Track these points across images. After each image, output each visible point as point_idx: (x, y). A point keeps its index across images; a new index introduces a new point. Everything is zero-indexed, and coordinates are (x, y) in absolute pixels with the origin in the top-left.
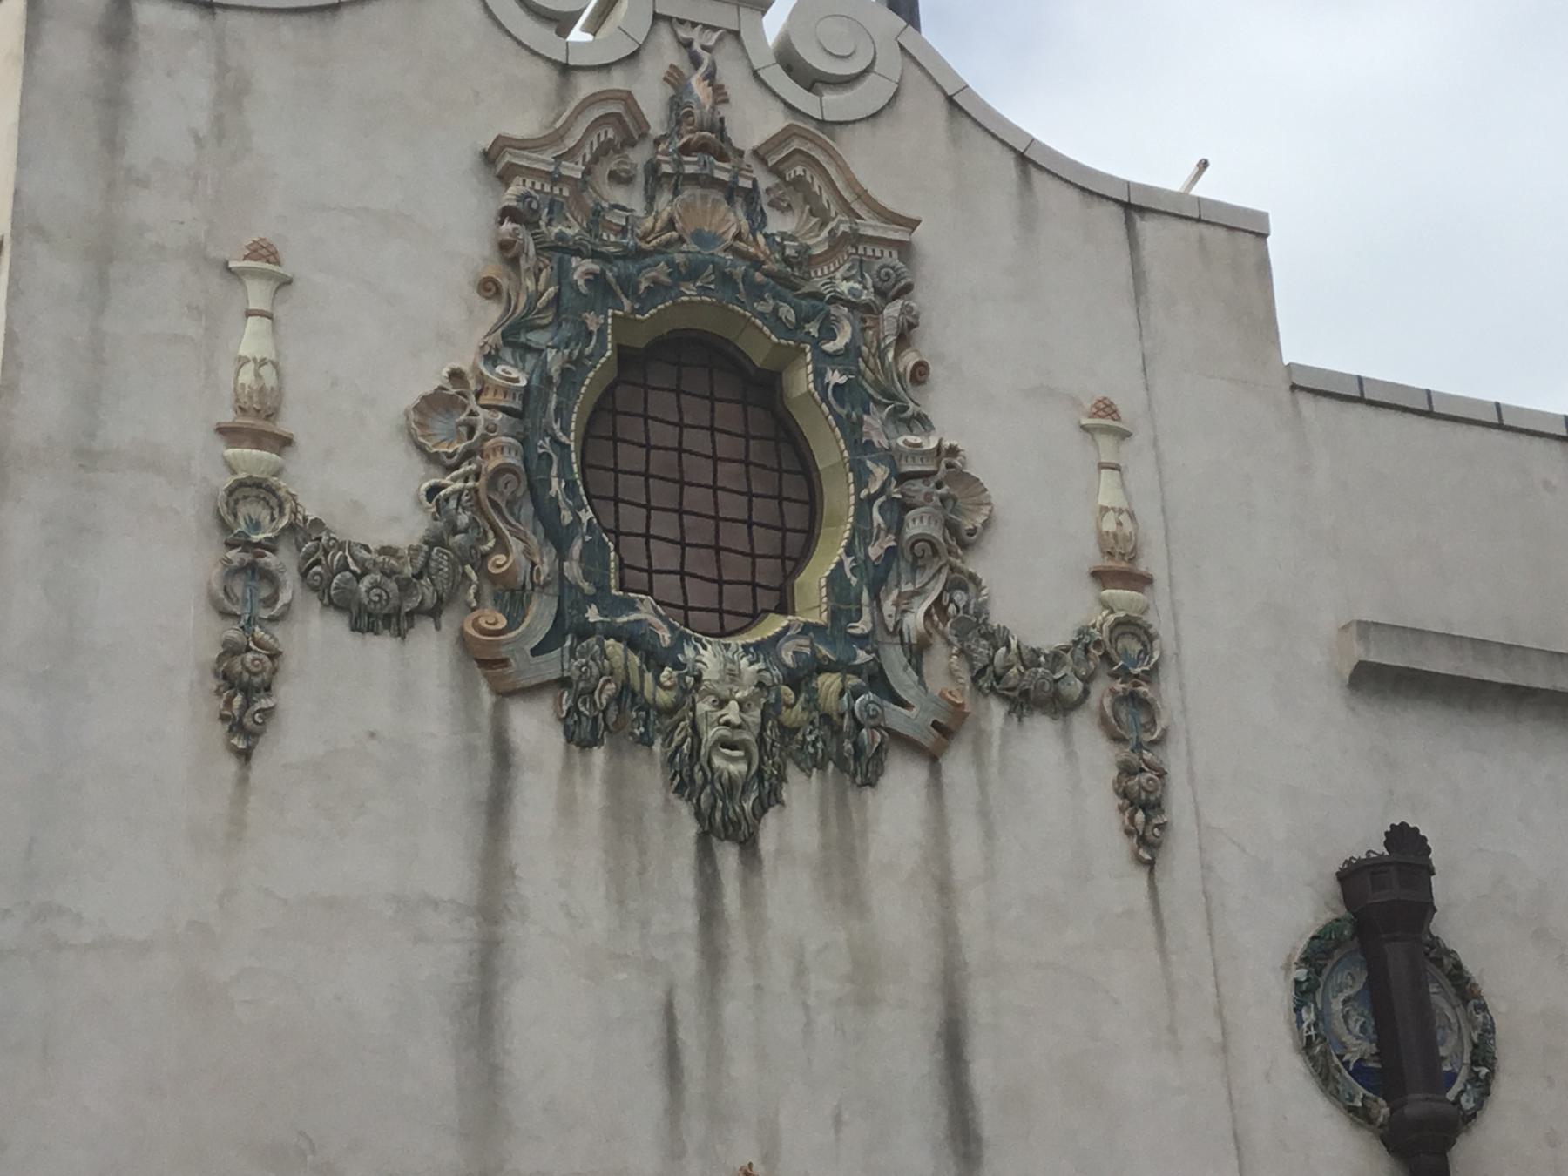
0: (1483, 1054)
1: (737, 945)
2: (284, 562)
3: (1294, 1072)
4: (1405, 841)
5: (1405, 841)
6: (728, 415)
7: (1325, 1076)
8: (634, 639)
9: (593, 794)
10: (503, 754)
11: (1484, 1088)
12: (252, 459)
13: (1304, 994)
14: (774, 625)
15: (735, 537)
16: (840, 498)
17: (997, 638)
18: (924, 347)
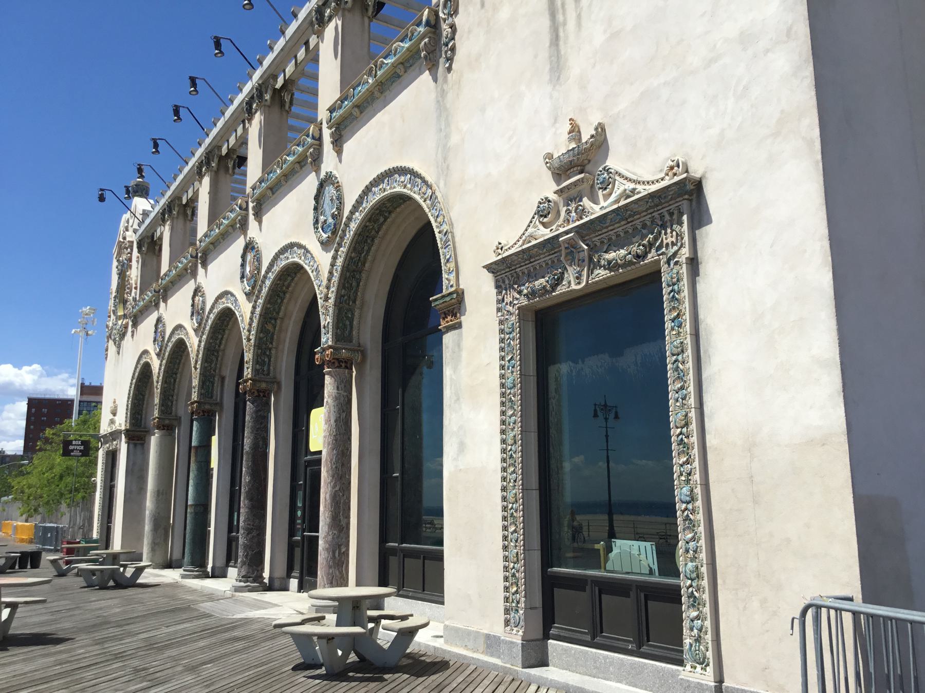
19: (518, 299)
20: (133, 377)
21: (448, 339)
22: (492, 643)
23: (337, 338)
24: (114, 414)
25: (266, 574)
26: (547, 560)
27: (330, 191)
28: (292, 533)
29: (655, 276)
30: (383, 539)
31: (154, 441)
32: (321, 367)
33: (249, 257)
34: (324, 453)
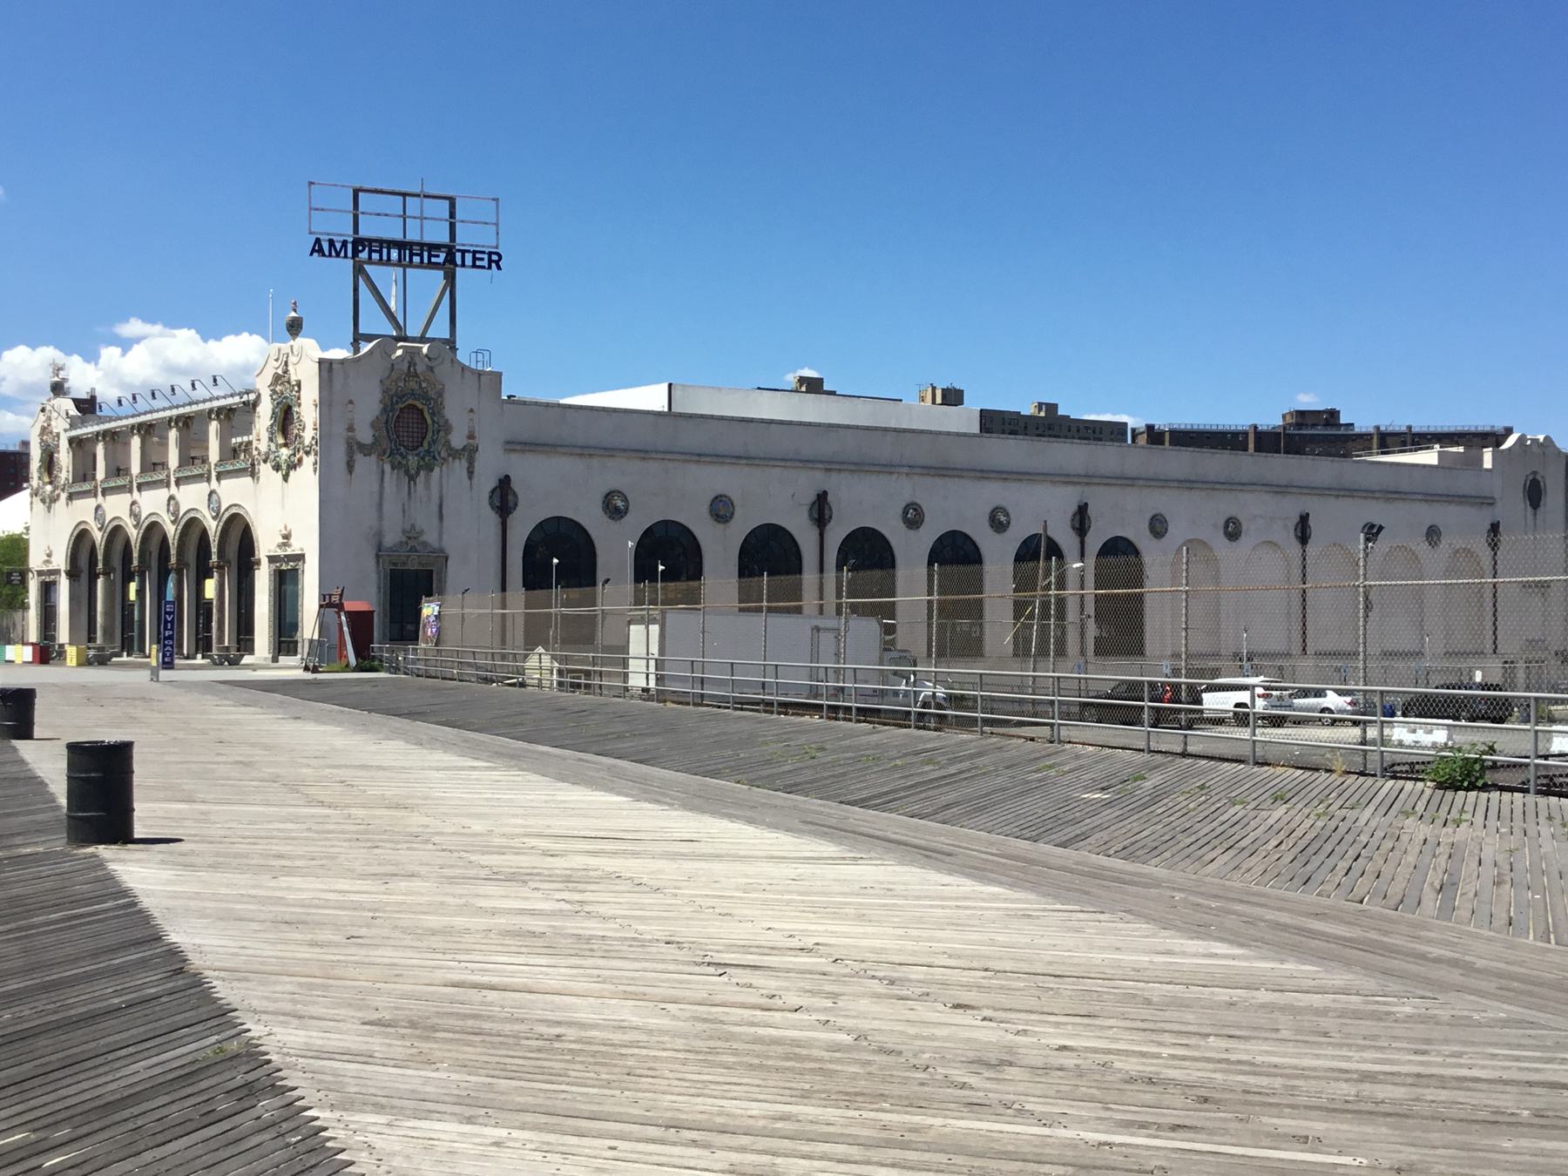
0: (516, 505)
1: (413, 495)
2: (355, 447)
3: (488, 508)
4: (507, 477)
5: (507, 477)
6: (415, 416)
7: (493, 509)
8: (401, 454)
9: (395, 476)
10: (383, 472)
11: (515, 509)
12: (350, 434)
13: (491, 497)
14: (420, 449)
15: (415, 435)
16: (430, 427)
17: (452, 449)
18: (445, 403)
19: (273, 566)
20: (71, 535)
21: (256, 572)
22: (266, 659)
23: (219, 557)
24: (49, 555)
25: (185, 652)
26: (280, 636)
27: (214, 496)
28: (197, 634)
29: (297, 570)
30: (238, 635)
31: (100, 582)
32: (213, 567)
33: (172, 502)
34: (214, 602)
